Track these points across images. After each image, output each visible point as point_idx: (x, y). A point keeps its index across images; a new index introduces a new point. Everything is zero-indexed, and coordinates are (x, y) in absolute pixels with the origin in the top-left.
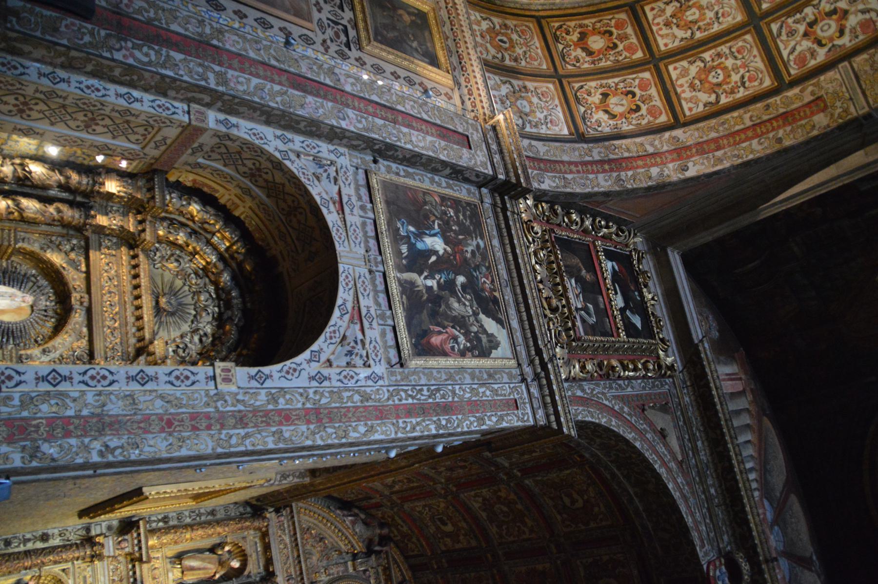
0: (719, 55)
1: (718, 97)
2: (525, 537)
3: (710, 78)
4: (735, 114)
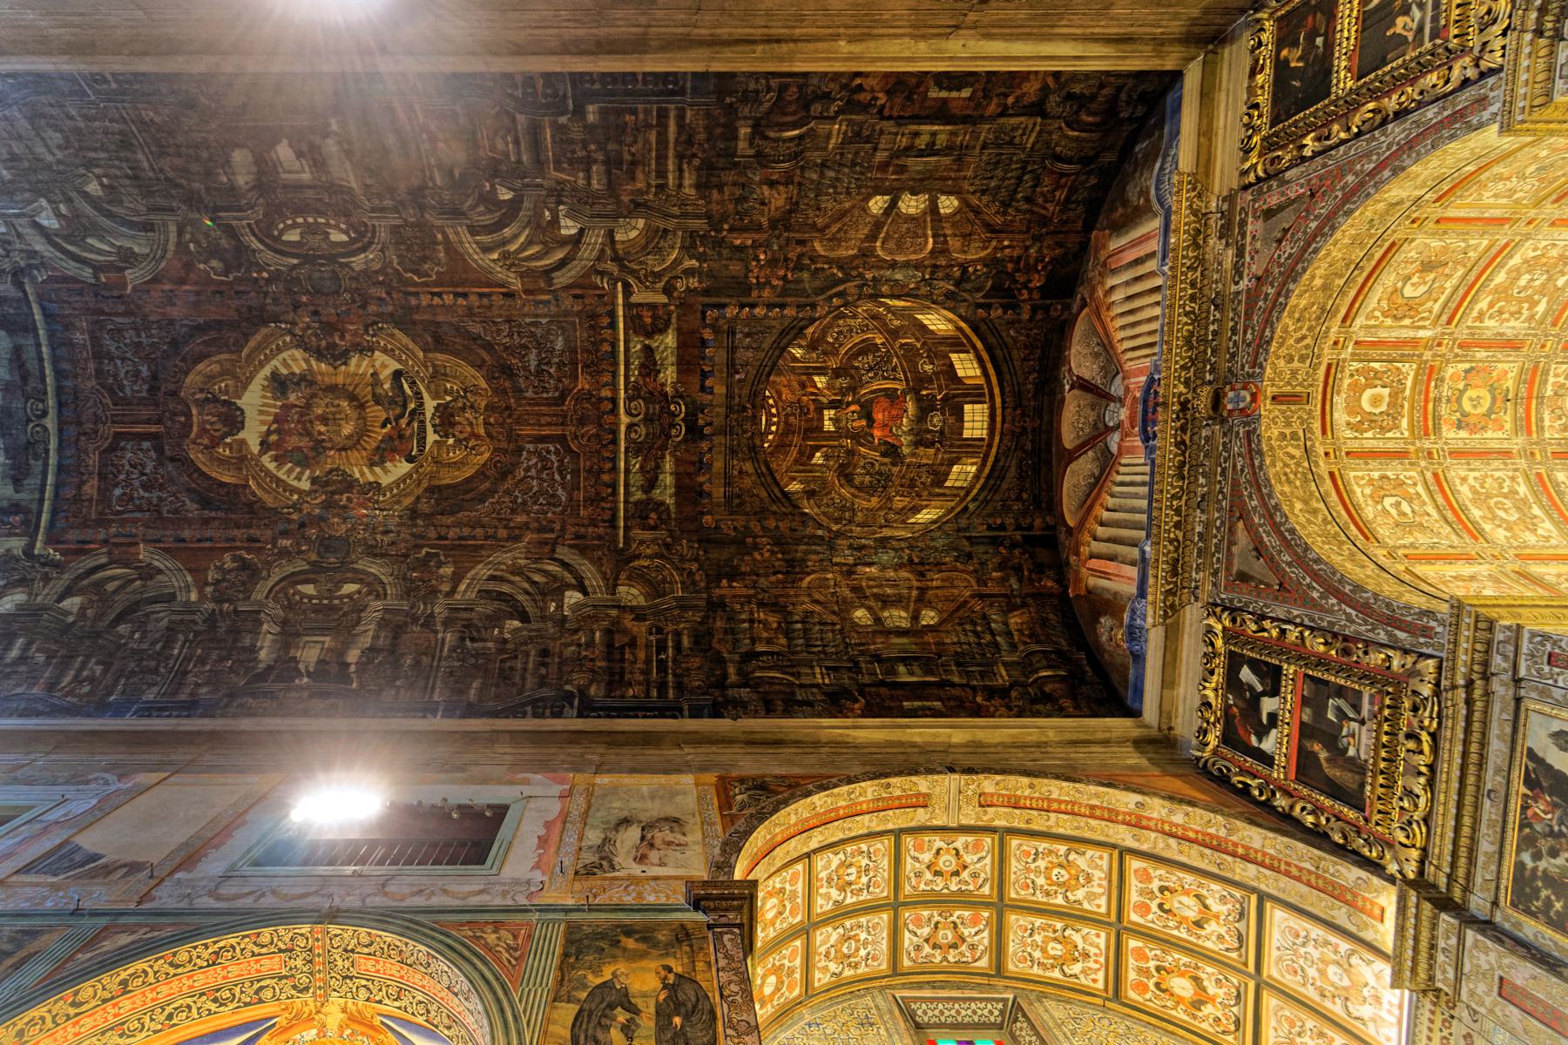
0: (1048, 894)
1: (1067, 856)
2: (1477, 474)
3: (1067, 876)
4: (1061, 831)
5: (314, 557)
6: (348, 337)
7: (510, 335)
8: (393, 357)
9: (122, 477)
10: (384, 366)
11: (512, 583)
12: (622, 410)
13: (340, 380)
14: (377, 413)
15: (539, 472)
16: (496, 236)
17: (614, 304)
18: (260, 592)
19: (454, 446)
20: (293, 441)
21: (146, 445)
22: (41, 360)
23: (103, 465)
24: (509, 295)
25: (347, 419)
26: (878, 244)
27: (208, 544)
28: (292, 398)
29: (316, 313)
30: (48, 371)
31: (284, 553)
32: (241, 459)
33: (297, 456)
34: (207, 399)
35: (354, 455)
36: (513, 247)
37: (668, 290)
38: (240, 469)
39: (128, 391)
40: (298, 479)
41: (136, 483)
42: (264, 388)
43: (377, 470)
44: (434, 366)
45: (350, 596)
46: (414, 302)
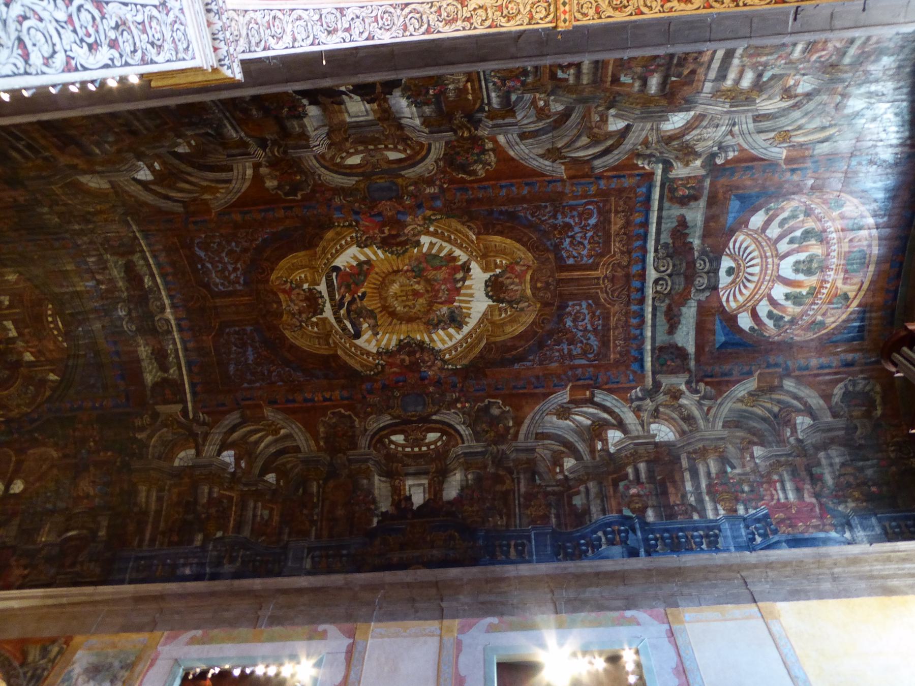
5: (400, 181)
6: (398, 362)
7: (270, 372)
8: (361, 349)
9: (590, 234)
10: (369, 341)
11: (206, 180)
12: (173, 322)
13: (404, 327)
14: (371, 303)
15: (225, 269)
16: (280, 446)
17: (194, 402)
18: (437, 150)
19: (302, 282)
20: (441, 275)
21: (571, 261)
22: (654, 326)
23: (607, 242)
24: (272, 402)
25: (396, 297)
26: (14, 459)
27: (503, 183)
28: (444, 310)
29: (423, 379)
30: (649, 317)
31: (430, 182)
32: (485, 257)
33: (437, 263)
34: (518, 303)
35: (386, 268)
36: (270, 438)
37: (155, 415)
38: (486, 248)
39: (584, 304)
40: (432, 245)
41: (577, 229)
42: (469, 315)
43: (363, 258)
44: (328, 344)
45: (350, 155)
46: (345, 394)
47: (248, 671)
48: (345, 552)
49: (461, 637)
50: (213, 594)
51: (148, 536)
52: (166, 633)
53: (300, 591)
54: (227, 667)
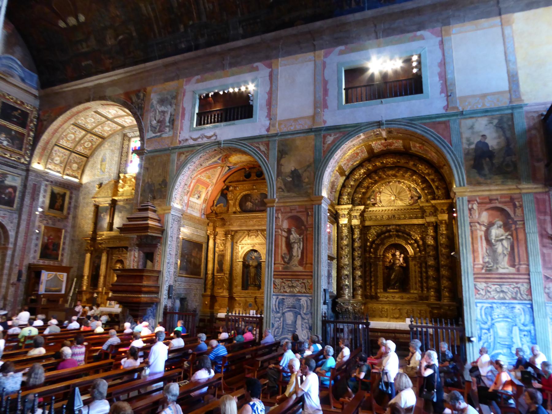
47: (226, 92)
48: (258, 20)
49: (325, 60)
50: (199, 57)
51: (156, 31)
52: (185, 79)
53: (240, 48)
54: (216, 91)
